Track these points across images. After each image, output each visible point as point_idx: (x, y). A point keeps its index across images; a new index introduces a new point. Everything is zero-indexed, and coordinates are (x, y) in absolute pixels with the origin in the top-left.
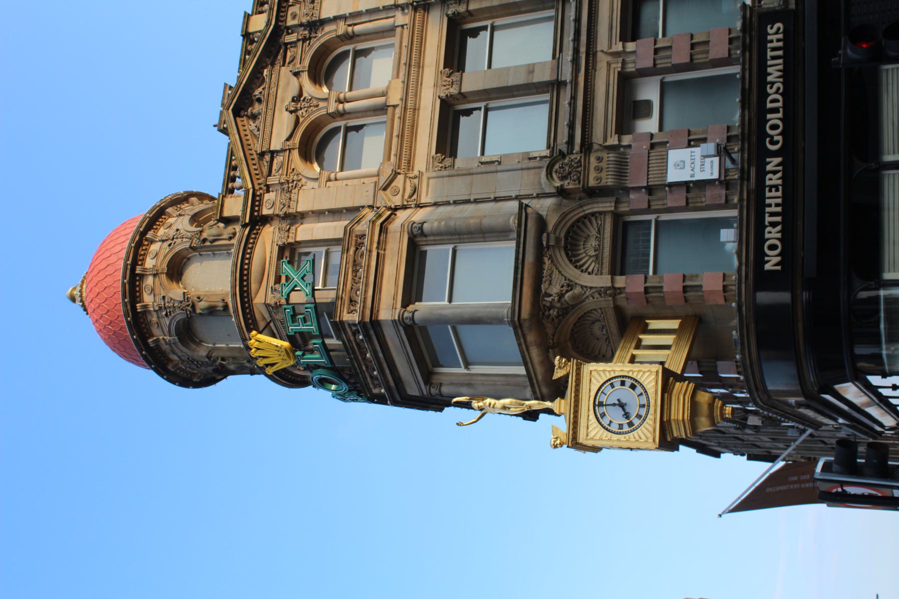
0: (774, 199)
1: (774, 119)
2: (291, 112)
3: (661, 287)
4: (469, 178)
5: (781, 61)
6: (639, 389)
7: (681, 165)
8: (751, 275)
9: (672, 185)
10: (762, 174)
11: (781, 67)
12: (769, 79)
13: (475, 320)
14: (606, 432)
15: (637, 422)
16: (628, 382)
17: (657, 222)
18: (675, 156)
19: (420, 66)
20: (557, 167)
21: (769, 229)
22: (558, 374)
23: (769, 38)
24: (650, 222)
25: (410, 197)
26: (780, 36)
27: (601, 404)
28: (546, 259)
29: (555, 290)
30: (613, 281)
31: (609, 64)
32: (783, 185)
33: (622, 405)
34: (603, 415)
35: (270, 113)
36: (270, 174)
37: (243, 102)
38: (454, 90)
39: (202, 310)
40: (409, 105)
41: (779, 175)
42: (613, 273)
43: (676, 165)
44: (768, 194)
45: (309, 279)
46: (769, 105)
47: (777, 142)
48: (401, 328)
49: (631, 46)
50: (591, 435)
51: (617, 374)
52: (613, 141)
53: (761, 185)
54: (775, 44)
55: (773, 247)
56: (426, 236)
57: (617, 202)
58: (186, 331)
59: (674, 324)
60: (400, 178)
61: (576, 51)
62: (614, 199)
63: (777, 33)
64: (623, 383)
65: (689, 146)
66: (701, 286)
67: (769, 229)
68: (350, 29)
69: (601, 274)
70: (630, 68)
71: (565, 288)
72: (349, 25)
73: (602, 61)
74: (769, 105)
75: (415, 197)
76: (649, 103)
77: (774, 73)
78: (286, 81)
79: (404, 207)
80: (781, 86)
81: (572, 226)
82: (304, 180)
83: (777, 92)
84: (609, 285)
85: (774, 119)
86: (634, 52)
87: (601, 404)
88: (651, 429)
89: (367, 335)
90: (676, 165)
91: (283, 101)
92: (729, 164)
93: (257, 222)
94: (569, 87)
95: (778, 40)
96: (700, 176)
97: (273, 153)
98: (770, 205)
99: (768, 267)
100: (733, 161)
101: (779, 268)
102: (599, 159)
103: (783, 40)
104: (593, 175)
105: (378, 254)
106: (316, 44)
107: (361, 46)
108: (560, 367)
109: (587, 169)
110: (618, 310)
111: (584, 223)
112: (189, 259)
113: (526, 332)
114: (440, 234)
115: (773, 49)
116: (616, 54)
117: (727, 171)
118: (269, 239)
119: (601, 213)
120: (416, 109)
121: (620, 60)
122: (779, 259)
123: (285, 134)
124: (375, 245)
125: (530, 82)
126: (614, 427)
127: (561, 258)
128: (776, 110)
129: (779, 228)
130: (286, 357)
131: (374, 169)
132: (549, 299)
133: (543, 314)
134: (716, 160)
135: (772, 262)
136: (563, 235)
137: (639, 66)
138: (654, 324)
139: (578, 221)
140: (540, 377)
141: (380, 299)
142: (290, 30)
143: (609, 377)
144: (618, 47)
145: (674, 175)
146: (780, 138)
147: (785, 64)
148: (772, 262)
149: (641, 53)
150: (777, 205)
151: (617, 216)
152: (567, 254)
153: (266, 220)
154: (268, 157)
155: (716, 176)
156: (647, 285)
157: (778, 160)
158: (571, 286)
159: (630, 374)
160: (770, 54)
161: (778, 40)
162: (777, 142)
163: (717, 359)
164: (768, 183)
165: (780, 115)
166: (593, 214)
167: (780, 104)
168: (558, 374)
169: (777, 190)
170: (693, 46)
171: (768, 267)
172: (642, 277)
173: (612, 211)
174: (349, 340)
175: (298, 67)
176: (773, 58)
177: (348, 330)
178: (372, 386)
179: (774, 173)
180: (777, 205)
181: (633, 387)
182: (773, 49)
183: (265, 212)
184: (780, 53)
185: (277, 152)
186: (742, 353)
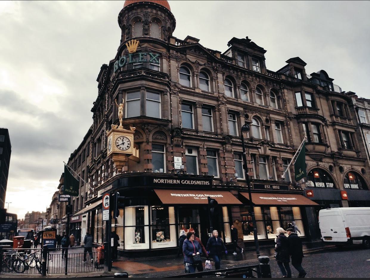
0: (170, 181)
1: (188, 182)
2: (196, 62)
3: (149, 154)
4: (177, 107)
5: (201, 184)
6: (127, 148)
7: (178, 160)
8: (153, 176)
9: (173, 158)
10: (176, 179)
11: (200, 184)
12: (197, 181)
13: (143, 106)
14: (116, 139)
15: (119, 147)
16: (129, 145)
17: (163, 153)
18: (180, 159)
19: (204, 98)
20: (179, 130)
21: (163, 180)
22: (131, 128)
23: (206, 182)
25: (173, 92)
26: (206, 184)
28: (157, 126)
29: (149, 127)
30: (150, 142)
31: (201, 144)
32: (173, 184)
33: (123, 144)
34: (121, 139)
41: (176, 183)
42: (152, 142)
43: (178, 159)
44: (171, 180)
45: (154, 62)
46: (191, 181)
47: (183, 183)
48: (140, 86)
49: (205, 150)
50: (115, 135)
51: (131, 143)
52: (184, 144)
53: (173, 179)
54: (205, 183)
55: (159, 181)
56: (164, 95)
57: (169, 144)
59: (138, 156)
60: (178, 90)
62: (170, 143)
63: (207, 183)
64: (129, 144)
65: (182, 162)
67: (163, 180)
69: (152, 139)
70: (200, 149)
71: (149, 130)
74: (191, 181)
75: (173, 93)
76: (191, 153)
77: (199, 183)
79: (170, 90)
80: (196, 184)
81: (164, 133)
82: (178, 63)
83: (194, 183)
84: (150, 141)
85: (188, 182)
86: (204, 150)
88: (117, 151)
90: (178, 159)
91: (198, 59)
94: (197, 134)
95: (206, 184)
96: (175, 164)
97: (186, 55)
98: (169, 181)
99: (155, 180)
100: (178, 172)
101: (154, 182)
102: (180, 141)
103: (206, 185)
104: (177, 139)
108: (133, 128)
109: (178, 138)
110: (142, 143)
111: (165, 136)
115: (204, 182)
116: (204, 147)
117: (176, 171)
119: (167, 140)
120: (194, 96)
121: (202, 147)
122: (156, 182)
123: (190, 59)
126: (117, 141)
127: (158, 129)
128: (190, 183)
129: (164, 182)
131: (180, 82)
132: (147, 126)
134: (180, 168)
135: (156, 181)
137: (201, 151)
138: (138, 151)
139: (165, 134)
143: (130, 141)
144: (205, 147)
145: (176, 158)
146: (184, 183)
147: (200, 185)
148: (156, 181)
149: (203, 152)
150: (169, 182)
151: (166, 144)
152: (158, 131)
153: (169, 51)
155: (175, 168)
156: (149, 151)
157: (179, 183)
158: (150, 131)
159: (131, 146)
160: (203, 182)
161: (206, 184)
162: (183, 183)
163: (128, 166)
164: (174, 180)
165: (189, 184)
166: (167, 138)
167: (192, 184)
168: (131, 128)
169: (172, 182)
170: (204, 164)
171: (155, 180)
172: (151, 149)
174: (137, 70)
175: (206, 65)
176: (202, 182)
177: (140, 71)
179: (176, 182)
180: (169, 182)
181: (128, 147)
182: (204, 182)
183: (171, 51)
184: (203, 184)
185: (186, 56)
186: (132, 173)
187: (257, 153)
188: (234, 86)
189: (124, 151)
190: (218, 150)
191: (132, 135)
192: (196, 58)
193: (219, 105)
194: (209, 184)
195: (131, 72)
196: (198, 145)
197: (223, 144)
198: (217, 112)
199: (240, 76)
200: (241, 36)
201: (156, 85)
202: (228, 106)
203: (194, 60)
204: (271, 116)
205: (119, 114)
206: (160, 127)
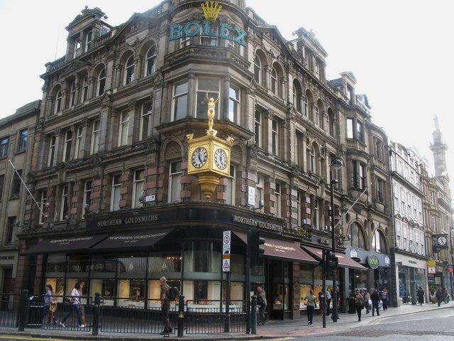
19: (275, 106)
37: (274, 34)
78: (276, 53)
89: (225, 60)
97: (261, 39)
119: (242, 160)
120: (266, 100)
142: (287, 59)
145: (250, 188)
151: (237, 165)
183: (249, 29)
187: (315, 194)
190: (283, 183)
193: (288, 119)
196: (267, 173)
197: (290, 176)
198: (285, 129)
200: (308, 29)
201: (240, 76)
202: (297, 124)
203: (268, 49)
205: (209, 112)
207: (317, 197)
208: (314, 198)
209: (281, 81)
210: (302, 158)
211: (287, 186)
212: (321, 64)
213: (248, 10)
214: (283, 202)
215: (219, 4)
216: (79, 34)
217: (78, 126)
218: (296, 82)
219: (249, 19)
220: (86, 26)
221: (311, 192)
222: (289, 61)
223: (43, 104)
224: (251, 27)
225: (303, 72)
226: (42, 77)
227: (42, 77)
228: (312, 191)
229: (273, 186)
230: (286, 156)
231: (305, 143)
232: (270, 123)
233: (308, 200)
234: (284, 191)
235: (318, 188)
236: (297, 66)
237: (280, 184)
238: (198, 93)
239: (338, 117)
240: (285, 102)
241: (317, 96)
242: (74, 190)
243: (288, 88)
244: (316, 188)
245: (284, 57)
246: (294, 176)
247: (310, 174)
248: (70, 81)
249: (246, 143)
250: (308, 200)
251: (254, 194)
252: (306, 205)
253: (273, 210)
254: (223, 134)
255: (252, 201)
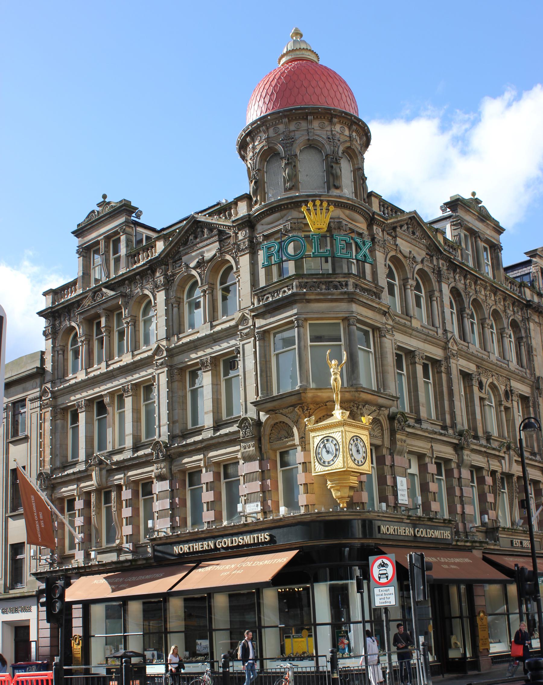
18: (404, 480)
19: (425, 341)
24: (442, 476)
27: (357, 440)
28: (375, 408)
35: (408, 239)
36: (388, 234)
38: (417, 360)
39: (336, 170)
40: (414, 333)
44: (403, 528)
56: (380, 338)
57: (387, 448)
58: (312, 146)
61: (435, 433)
66: (362, 490)
68: (435, 299)
70: (427, 460)
72: (437, 298)
73: (428, 445)
74: (428, 530)
78: (420, 253)
87: (357, 440)
89: (345, 292)
90: (402, 481)
91: (414, 250)
92: (403, 508)
93: (371, 221)
97: (395, 237)
100: (403, 511)
105: (376, 308)
106: (432, 276)
107: (423, 302)
112: (349, 161)
113: (352, 393)
114: (381, 347)
116: (433, 454)
117: (400, 507)
118: (362, 225)
119: (383, 438)
120: (410, 335)
121: (431, 456)
123: (402, 248)
124: (380, 307)
125: (421, 405)
130: (316, 226)
133: (356, 404)
136: (380, 418)
140: (320, 394)
141: (360, 305)
142: (437, 259)
145: (399, 479)
146: (419, 535)
153: (370, 226)
154: (393, 234)
155: (400, 502)
165: (425, 536)
166: (383, 434)
170: (434, 493)
173: (383, 445)
175: (426, 263)
177: (343, 280)
178: (300, 280)
179: (409, 532)
183: (375, 227)
185: (395, 241)
187: (500, 470)
188: (457, 310)
189: (360, 467)
190: (447, 461)
191: (367, 433)
192: (409, 245)
193: (447, 358)
194: (449, 538)
195: (322, 280)
197: (458, 448)
199: (470, 290)
204: (515, 384)
206: (379, 410)
207: (502, 473)
208: (498, 475)
209: (430, 297)
210: (474, 413)
211: (453, 465)
212: (495, 249)
213: (371, 195)
214: (450, 491)
215: (328, 201)
216: (98, 243)
217: (119, 396)
218: (455, 292)
219: (374, 213)
220: (109, 226)
221: (493, 468)
222: (441, 262)
223: (48, 358)
224: (378, 225)
225: (465, 273)
226: (40, 314)
227: (40, 314)
228: (495, 465)
229: (432, 468)
230: (448, 417)
231: (476, 389)
232: (419, 369)
233: (489, 480)
234: (449, 473)
235: (503, 458)
236: (454, 267)
237: (442, 463)
238: (311, 346)
239: (527, 330)
240: (440, 331)
241: (491, 303)
242: (123, 498)
243: (442, 307)
244: (500, 458)
245: (431, 256)
246: (462, 448)
247: (489, 438)
248: (91, 321)
249: (386, 412)
250: (489, 480)
251: (405, 487)
252: (486, 488)
253: (435, 506)
254: (354, 409)
255: (403, 498)
